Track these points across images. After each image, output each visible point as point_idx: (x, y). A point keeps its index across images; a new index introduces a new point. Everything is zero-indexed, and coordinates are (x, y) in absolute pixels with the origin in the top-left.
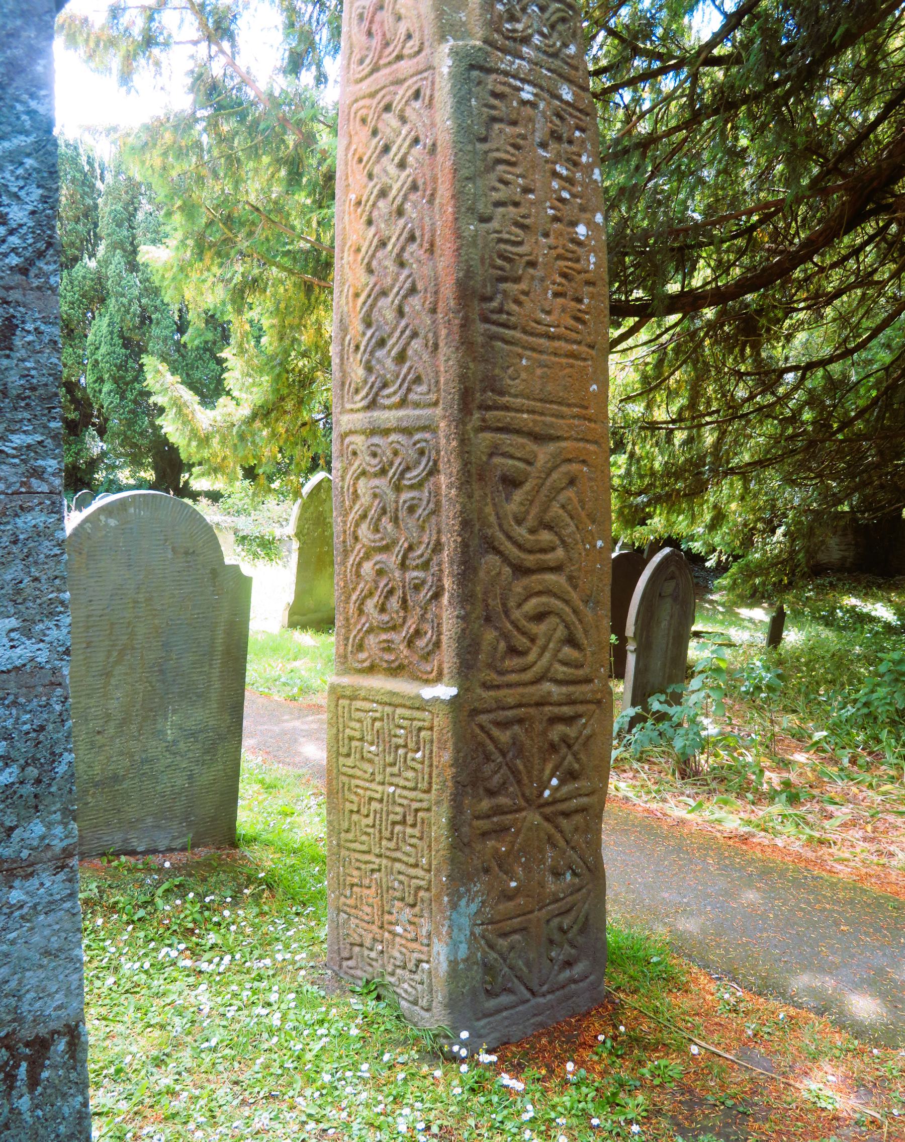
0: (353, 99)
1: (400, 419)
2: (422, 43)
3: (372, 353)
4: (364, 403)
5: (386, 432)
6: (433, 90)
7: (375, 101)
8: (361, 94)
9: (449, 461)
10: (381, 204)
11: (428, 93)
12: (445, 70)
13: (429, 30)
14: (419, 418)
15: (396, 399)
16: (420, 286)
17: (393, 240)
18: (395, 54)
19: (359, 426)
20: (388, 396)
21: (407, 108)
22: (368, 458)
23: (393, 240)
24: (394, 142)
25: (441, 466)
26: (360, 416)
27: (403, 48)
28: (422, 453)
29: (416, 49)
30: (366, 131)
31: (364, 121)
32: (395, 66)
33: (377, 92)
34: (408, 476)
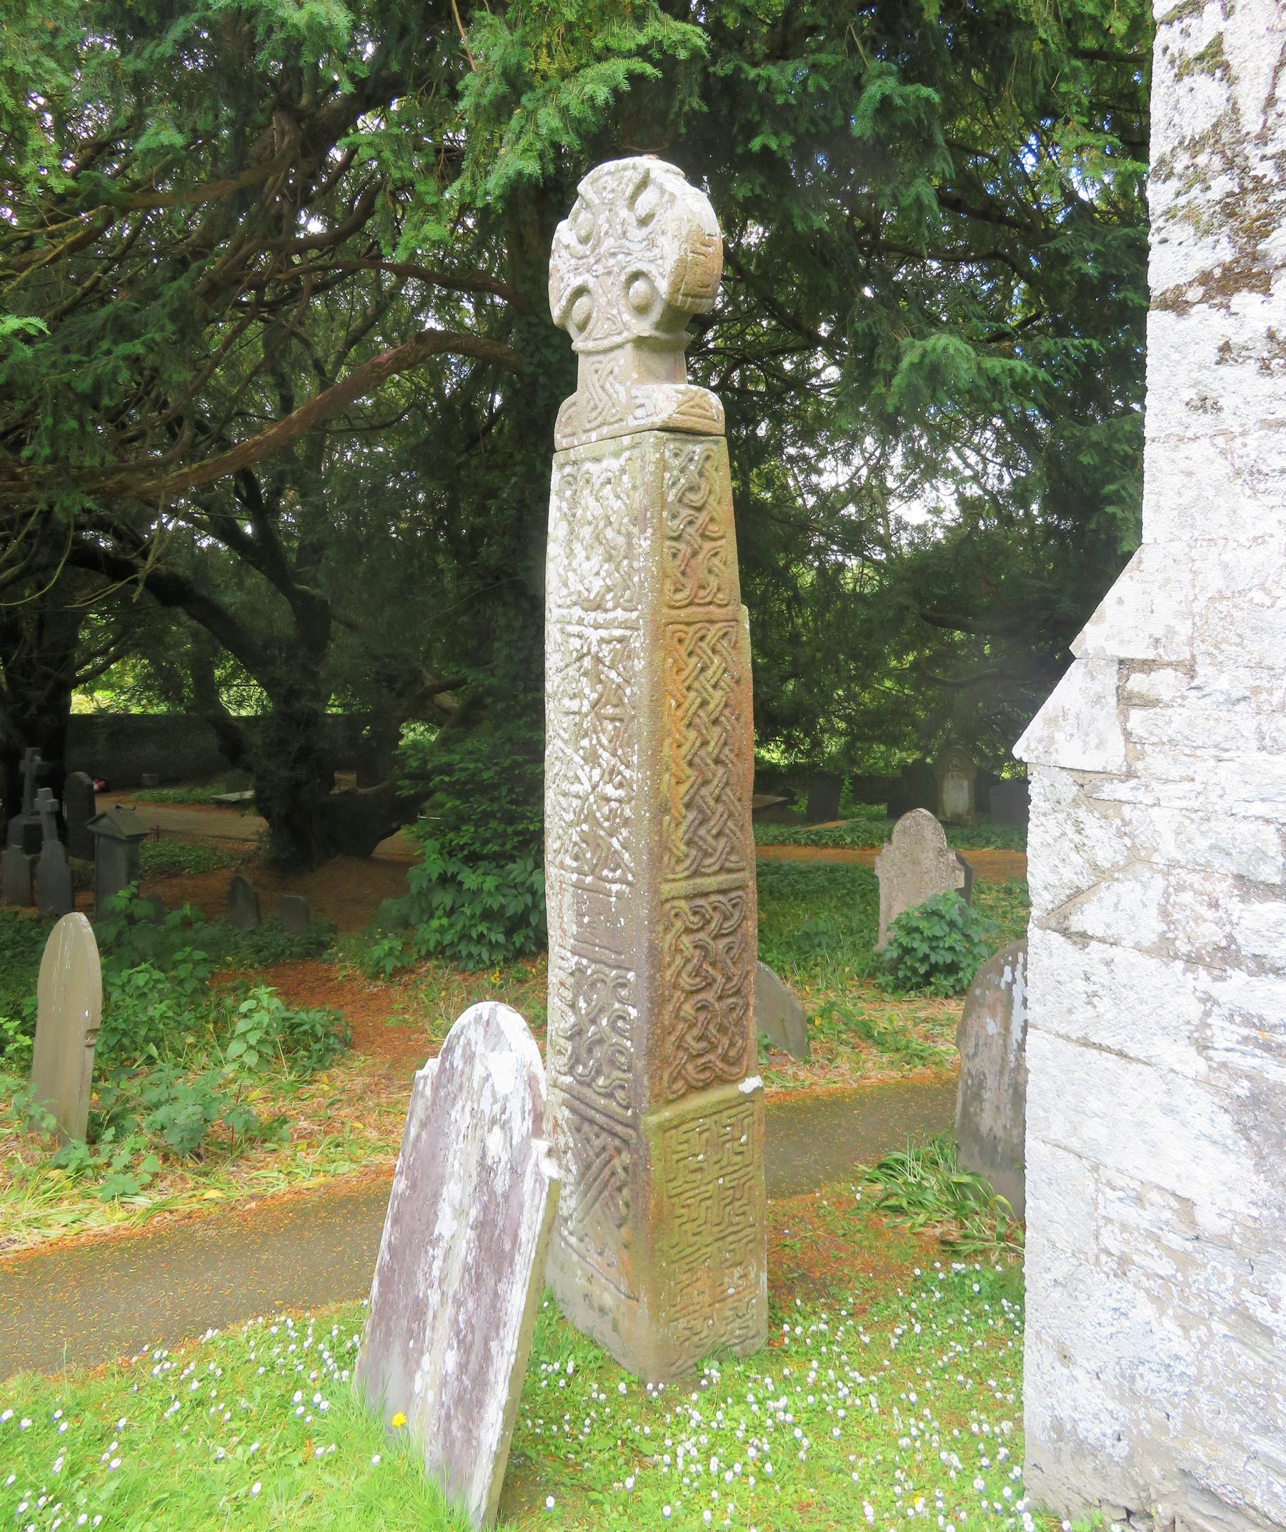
3: (695, 832)
4: (686, 873)
5: (705, 895)
7: (692, 629)
10: (702, 713)
15: (716, 867)
19: (683, 893)
26: (683, 884)
30: (683, 650)
31: (680, 641)
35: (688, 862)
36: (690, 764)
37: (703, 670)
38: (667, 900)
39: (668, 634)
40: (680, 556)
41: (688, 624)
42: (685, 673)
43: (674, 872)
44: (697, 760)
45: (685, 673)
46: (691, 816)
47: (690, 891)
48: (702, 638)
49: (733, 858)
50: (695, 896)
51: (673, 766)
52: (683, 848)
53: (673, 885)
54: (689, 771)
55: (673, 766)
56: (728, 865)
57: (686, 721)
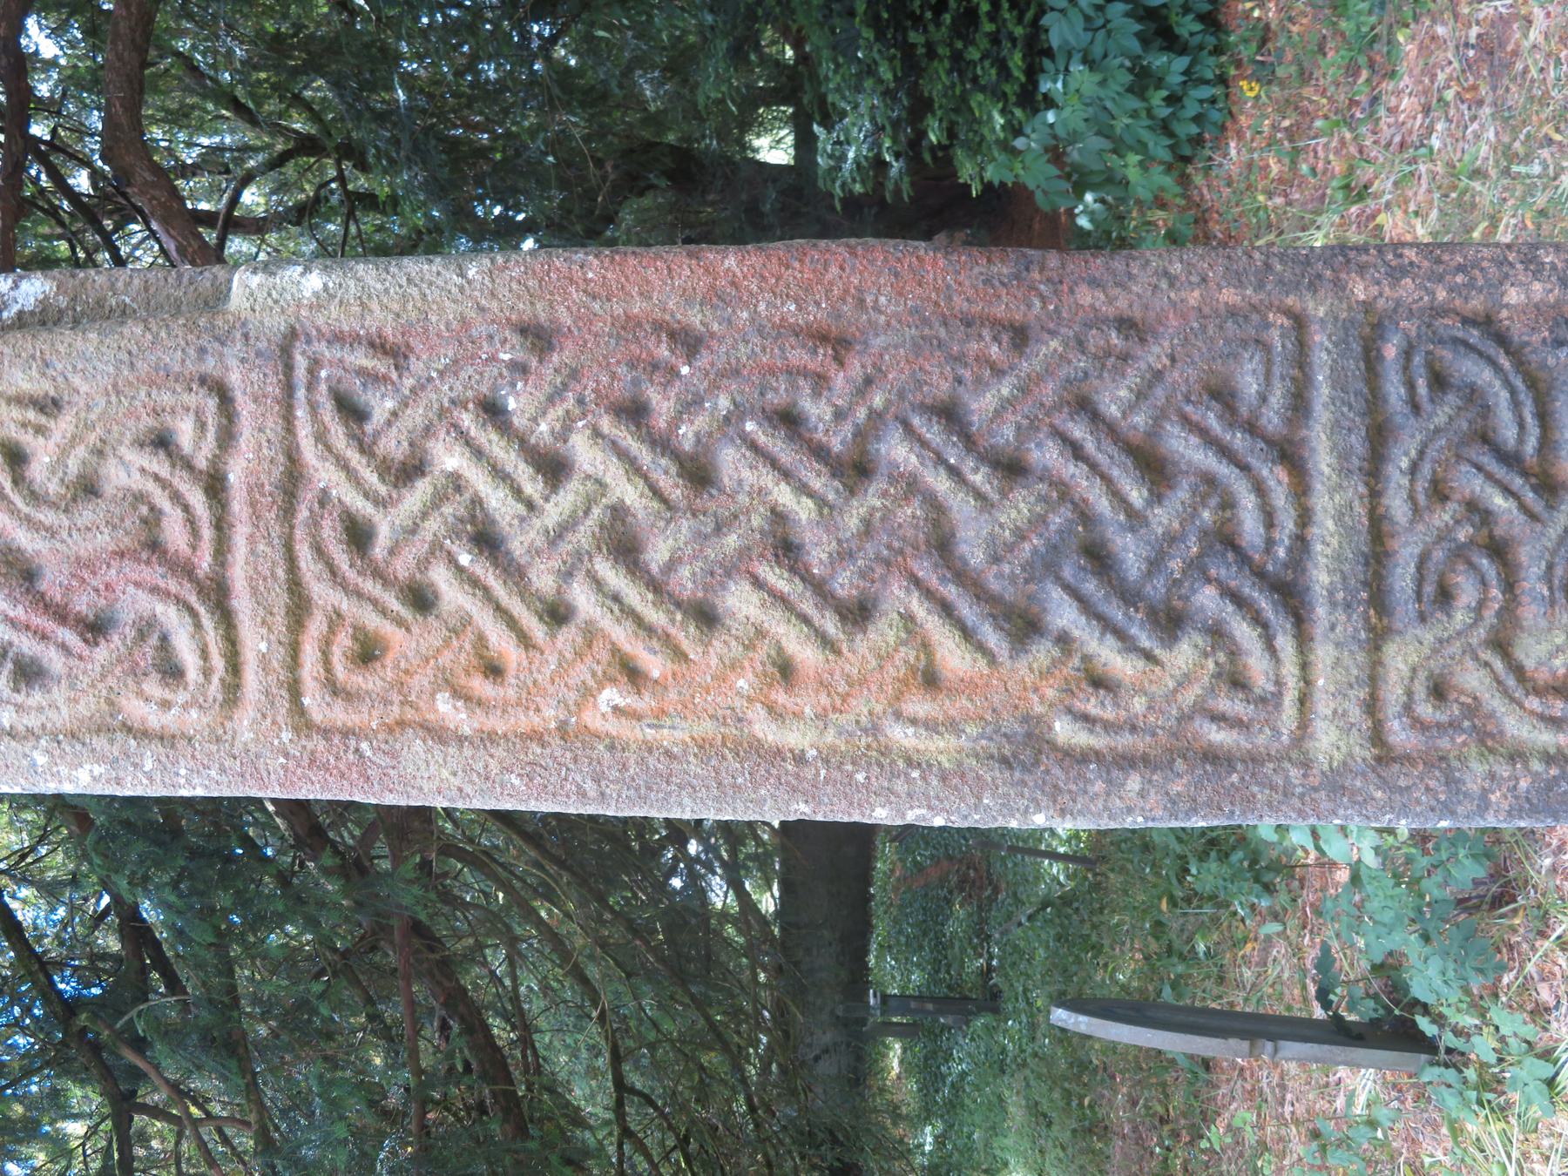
0: (283, 705)
1: (1344, 471)
2: (203, 381)
3: (1129, 596)
4: (1285, 644)
6: (353, 340)
7: (322, 593)
8: (279, 655)
9: (1461, 268)
10: (657, 554)
11: (361, 358)
12: (314, 282)
13: (172, 349)
14: (1338, 382)
15: (1277, 479)
16: (941, 387)
17: (784, 495)
18: (197, 499)
19: (1356, 661)
20: (1269, 518)
21: (380, 450)
22: (1460, 617)
23: (784, 495)
24: (477, 501)
25: (1476, 303)
26: (1323, 653)
27: (188, 466)
28: (1439, 381)
29: (212, 404)
30: (406, 642)
31: (368, 653)
32: (238, 506)
33: (295, 585)
34: (1509, 434)
35: (1244, 632)
36: (858, 613)
37: (487, 540)
38: (1377, 736)
39: (339, 714)
40: (26, 645)
41: (299, 608)
42: (500, 641)
43: (1269, 702)
44: (845, 584)
45: (500, 641)
46: (1064, 615)
47: (1350, 625)
48: (358, 535)
49: (1249, 383)
50: (1379, 598)
51: (861, 707)
52: (1184, 654)
53: (1323, 706)
54: (884, 631)
55: (861, 707)
56: (1272, 418)
57: (686, 636)
